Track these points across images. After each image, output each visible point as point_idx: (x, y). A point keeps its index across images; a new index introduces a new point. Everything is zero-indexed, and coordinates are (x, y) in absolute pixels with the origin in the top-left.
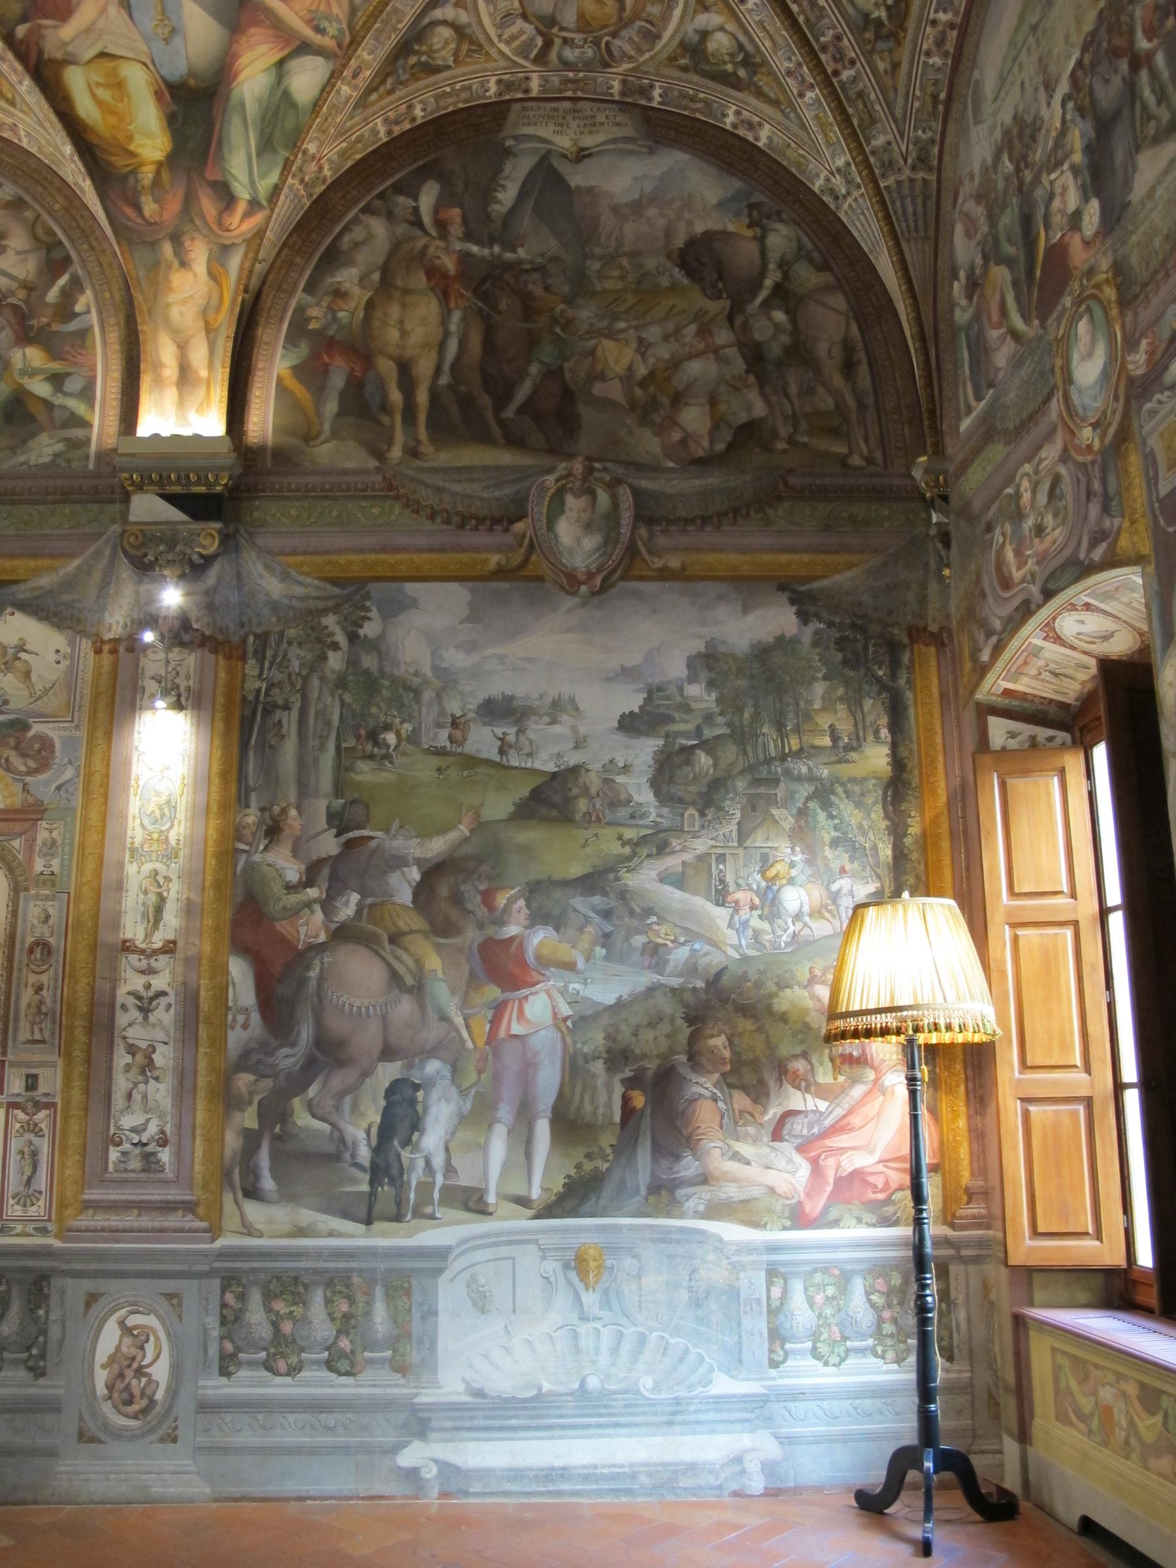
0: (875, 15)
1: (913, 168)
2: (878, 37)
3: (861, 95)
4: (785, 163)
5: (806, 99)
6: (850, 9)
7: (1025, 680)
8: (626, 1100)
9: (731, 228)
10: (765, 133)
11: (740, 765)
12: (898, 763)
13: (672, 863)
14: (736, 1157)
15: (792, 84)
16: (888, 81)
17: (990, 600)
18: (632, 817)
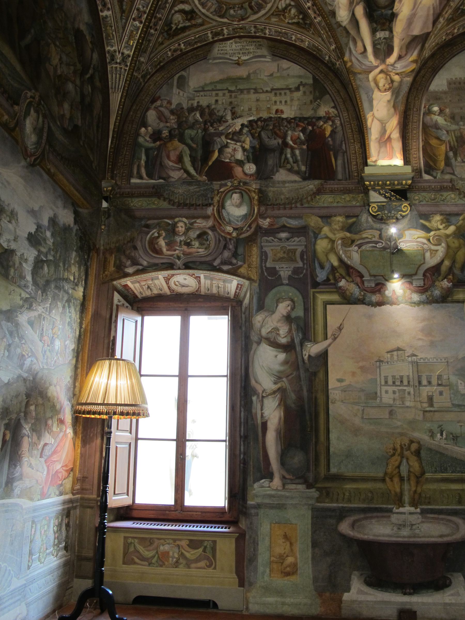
0: (173, 26)
1: (142, 77)
2: (167, 32)
3: (149, 41)
4: (103, 29)
5: (135, 23)
6: (170, 16)
7: (137, 285)
8: (4, 435)
9: (87, 37)
10: (105, 13)
11: (54, 277)
12: (84, 296)
13: (33, 314)
14: (31, 466)
15: (135, 14)
16: (157, 45)
17: (141, 252)
18: (25, 286)
